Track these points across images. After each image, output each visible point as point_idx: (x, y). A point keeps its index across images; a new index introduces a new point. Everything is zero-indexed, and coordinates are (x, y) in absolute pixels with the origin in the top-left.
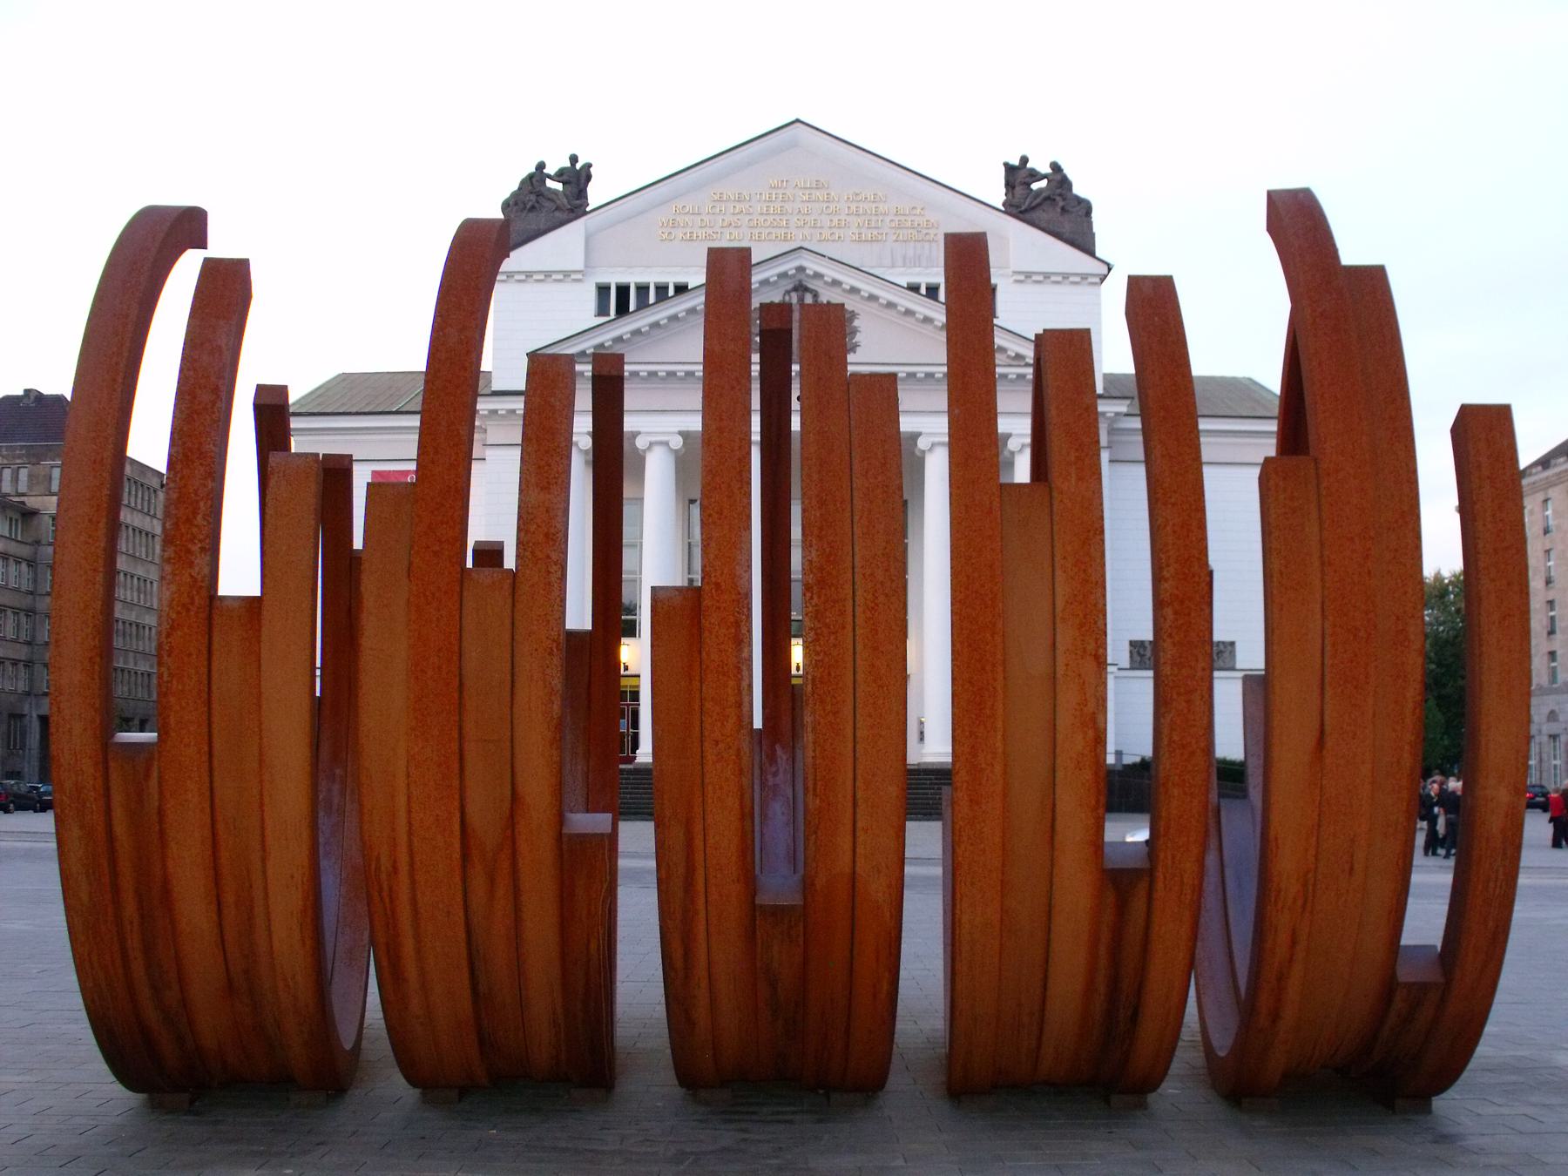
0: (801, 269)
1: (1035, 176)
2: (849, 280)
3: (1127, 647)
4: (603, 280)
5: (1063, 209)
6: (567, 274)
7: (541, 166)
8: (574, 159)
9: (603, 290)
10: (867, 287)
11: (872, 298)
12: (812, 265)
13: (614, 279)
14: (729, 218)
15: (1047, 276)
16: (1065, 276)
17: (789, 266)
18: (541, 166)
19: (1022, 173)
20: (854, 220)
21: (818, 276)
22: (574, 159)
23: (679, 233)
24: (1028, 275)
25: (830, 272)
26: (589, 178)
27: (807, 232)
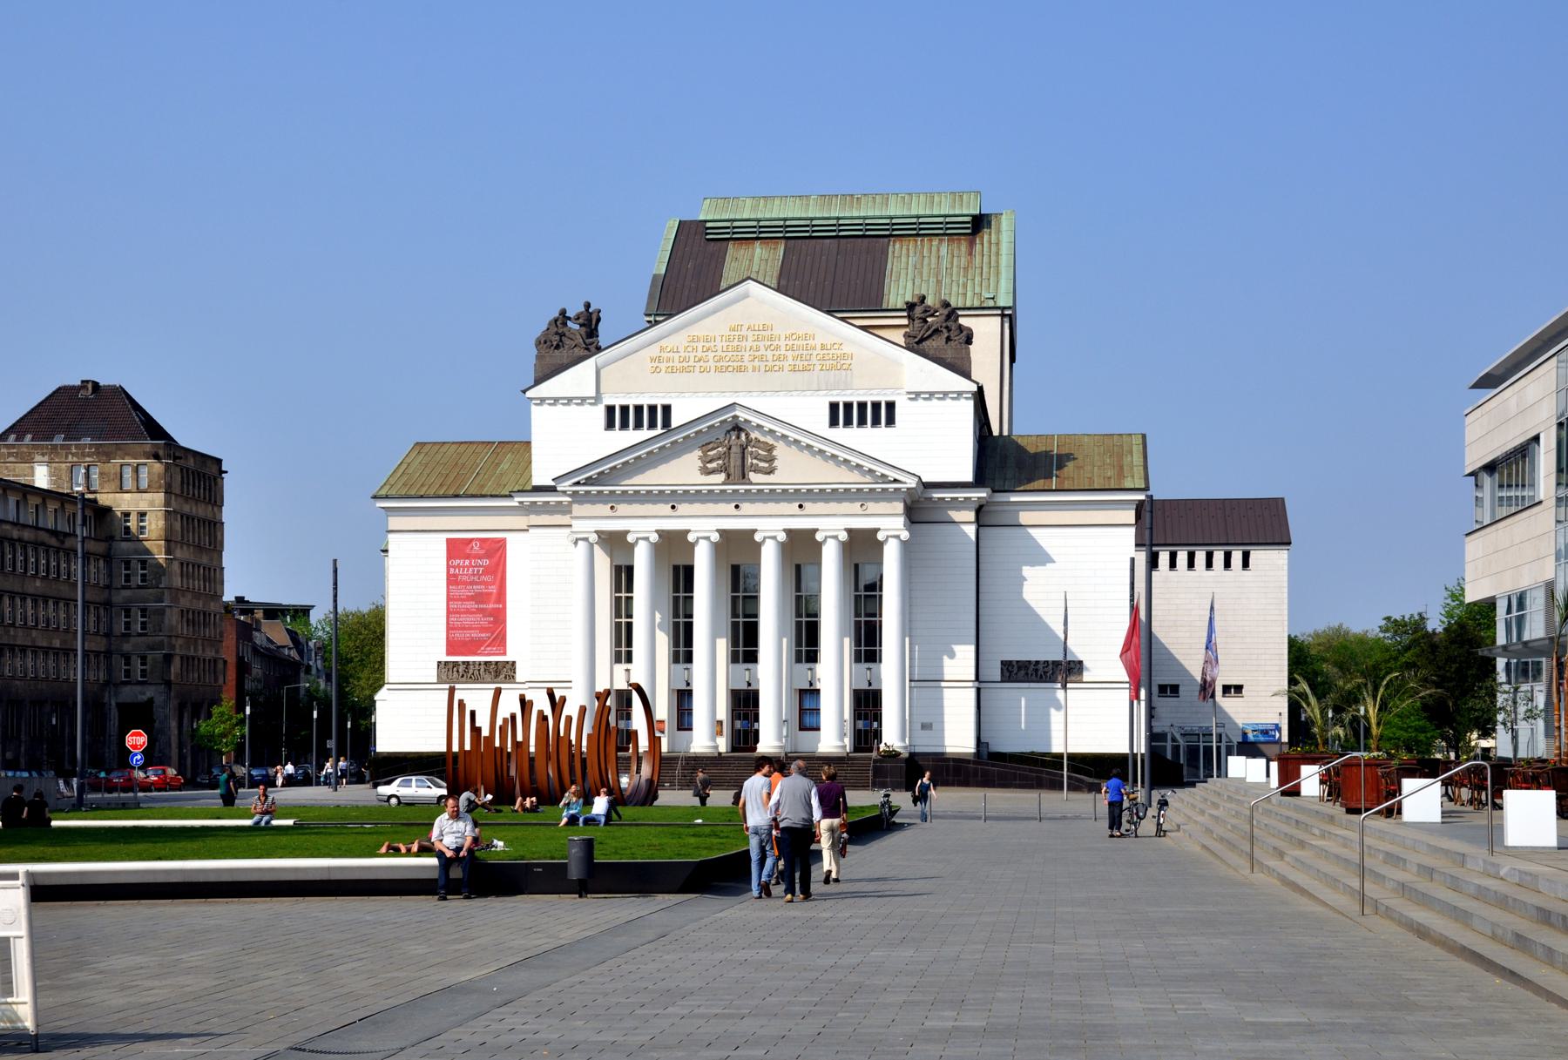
0: (735, 417)
1: (929, 311)
2: (768, 425)
3: (999, 665)
4: (610, 403)
5: (948, 339)
6: (583, 400)
7: (563, 312)
8: (588, 305)
9: (610, 410)
10: (780, 430)
11: (784, 437)
12: (743, 415)
13: (617, 402)
14: (700, 354)
15: (932, 394)
16: (946, 394)
17: (728, 416)
18: (563, 312)
19: (918, 310)
20: (790, 353)
21: (746, 421)
22: (588, 305)
23: (663, 366)
24: (918, 394)
25: (755, 420)
26: (599, 320)
27: (756, 363)
